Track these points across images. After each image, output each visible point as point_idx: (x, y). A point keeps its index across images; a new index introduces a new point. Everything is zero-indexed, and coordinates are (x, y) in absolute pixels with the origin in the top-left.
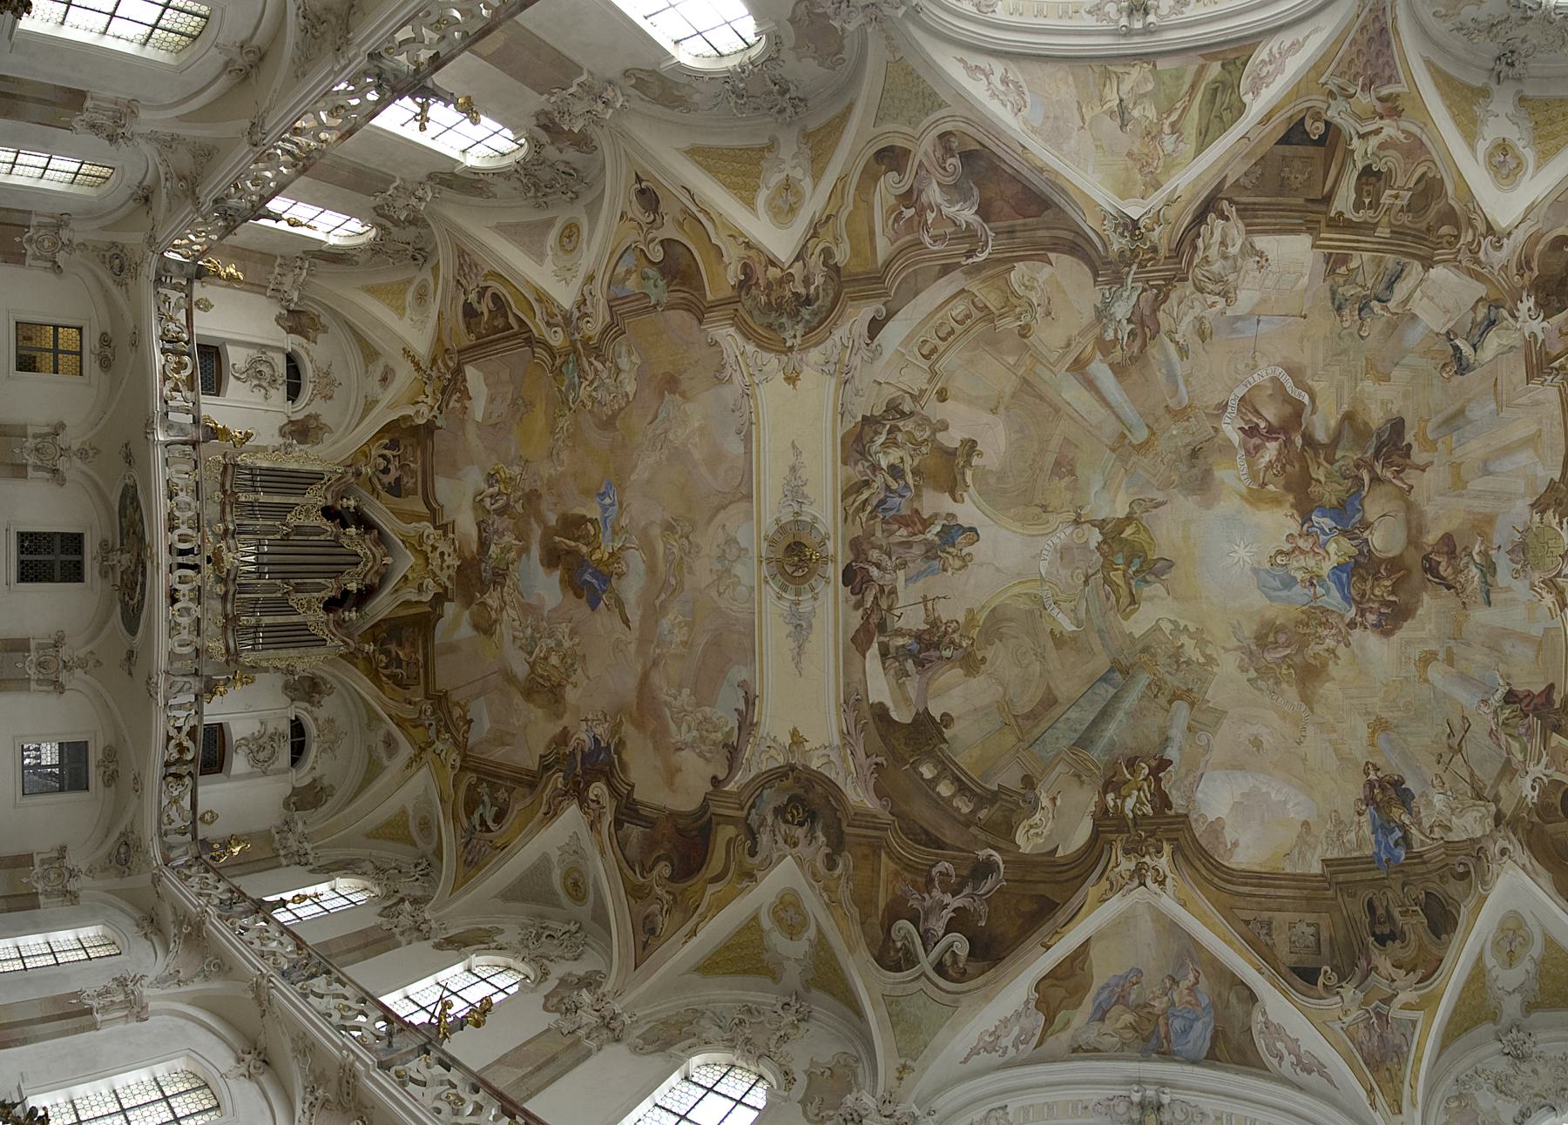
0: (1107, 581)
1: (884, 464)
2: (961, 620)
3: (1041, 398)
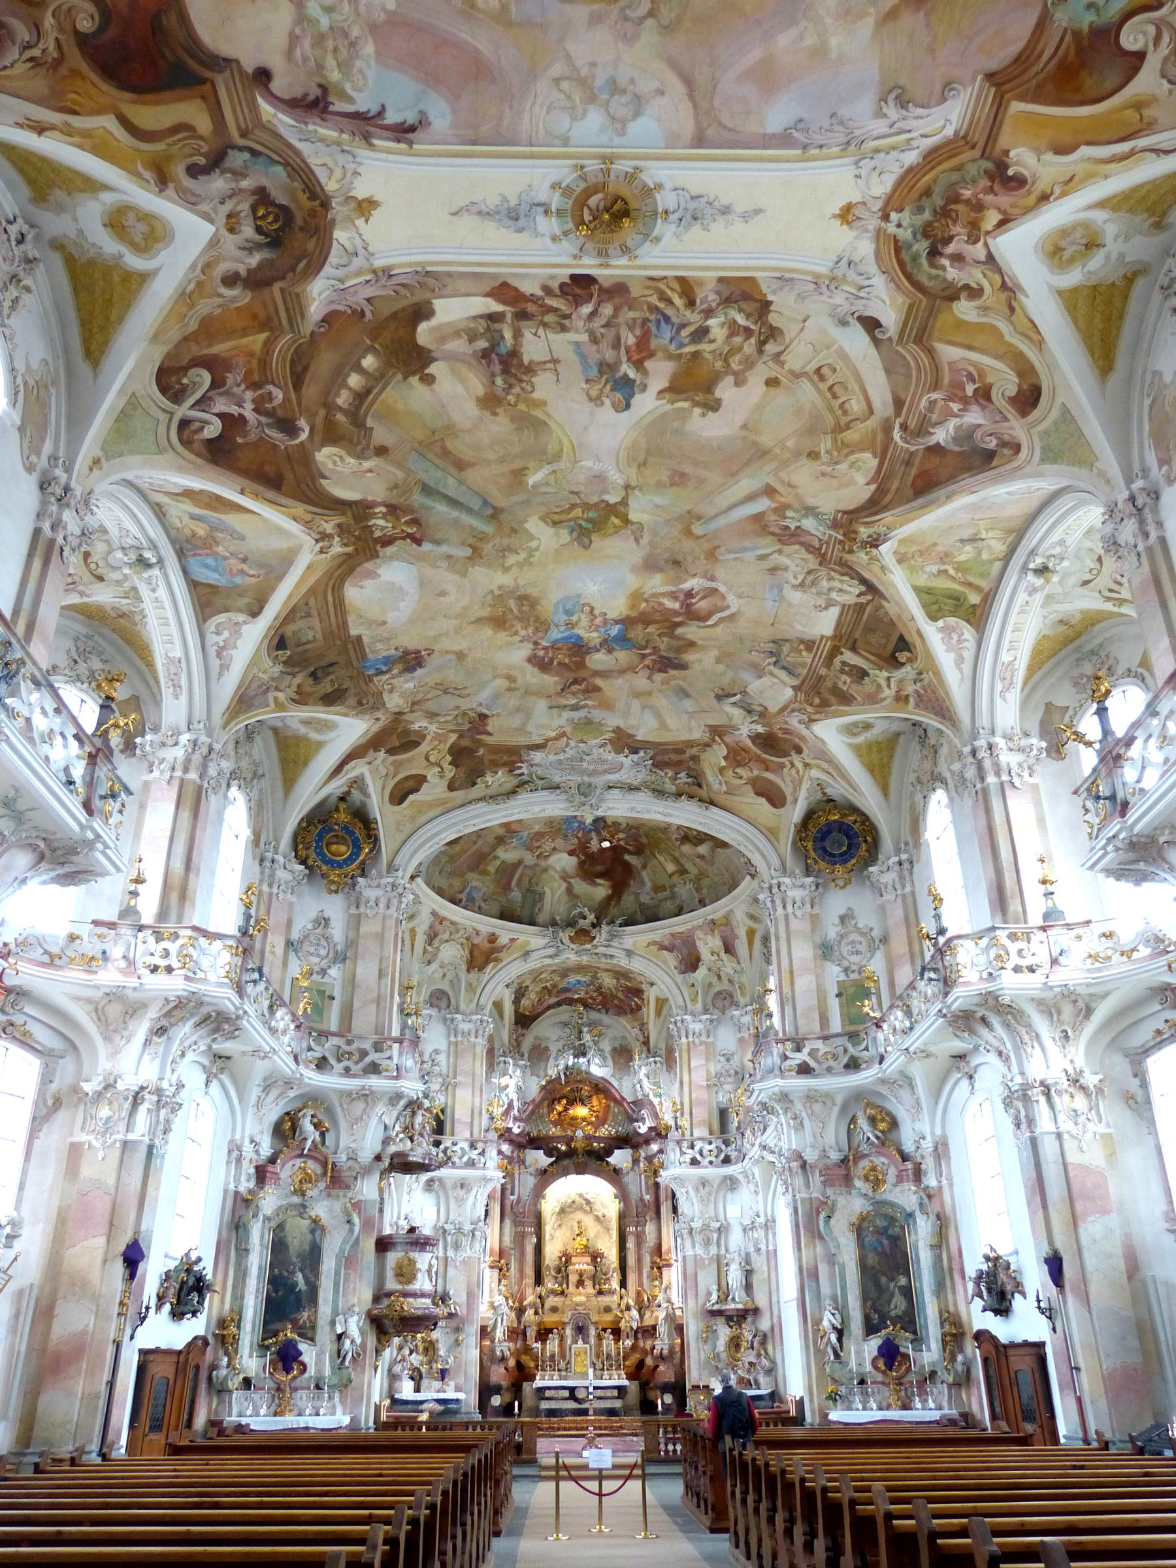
0: (573, 506)
1: (711, 322)
2: (536, 395)
3: (748, 463)
